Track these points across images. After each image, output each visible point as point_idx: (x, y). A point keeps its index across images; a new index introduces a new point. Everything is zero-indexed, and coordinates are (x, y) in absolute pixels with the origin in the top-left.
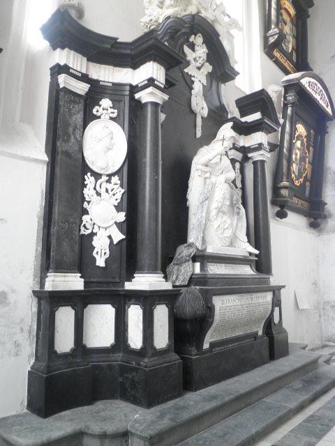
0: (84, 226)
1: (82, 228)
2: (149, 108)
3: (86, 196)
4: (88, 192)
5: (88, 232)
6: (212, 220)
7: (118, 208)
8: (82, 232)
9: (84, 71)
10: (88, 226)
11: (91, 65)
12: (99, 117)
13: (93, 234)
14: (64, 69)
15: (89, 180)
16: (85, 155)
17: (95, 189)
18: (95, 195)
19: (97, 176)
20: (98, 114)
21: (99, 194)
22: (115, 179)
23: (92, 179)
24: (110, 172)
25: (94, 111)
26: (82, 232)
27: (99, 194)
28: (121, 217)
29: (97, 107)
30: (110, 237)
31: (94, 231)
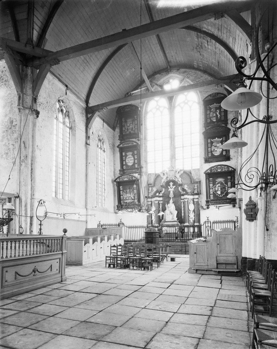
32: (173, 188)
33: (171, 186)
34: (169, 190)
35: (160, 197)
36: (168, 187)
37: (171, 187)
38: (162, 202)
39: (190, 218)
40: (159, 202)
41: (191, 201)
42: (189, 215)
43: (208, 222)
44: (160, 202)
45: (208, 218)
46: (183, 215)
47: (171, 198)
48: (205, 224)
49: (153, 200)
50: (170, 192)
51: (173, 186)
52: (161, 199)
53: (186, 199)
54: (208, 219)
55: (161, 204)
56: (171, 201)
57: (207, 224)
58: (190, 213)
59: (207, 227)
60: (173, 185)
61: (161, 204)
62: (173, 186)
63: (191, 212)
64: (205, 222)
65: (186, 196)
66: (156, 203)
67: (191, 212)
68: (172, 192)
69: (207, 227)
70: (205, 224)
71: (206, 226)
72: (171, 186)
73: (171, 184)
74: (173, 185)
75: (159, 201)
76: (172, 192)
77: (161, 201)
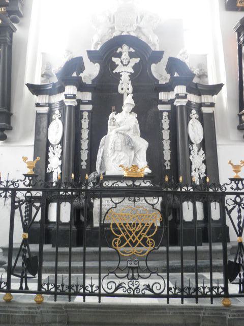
0: (49, 169)
2: (67, 108)
4: (50, 154)
5: (50, 171)
6: (110, 156)
7: (60, 159)
8: (47, 172)
9: (47, 102)
10: (50, 169)
11: (51, 97)
14: (38, 105)
15: (51, 149)
16: (49, 138)
21: (54, 154)
22: (60, 146)
23: (52, 148)
24: (57, 143)
26: (47, 172)
27: (54, 154)
28: (60, 163)
32: (132, 64)
33: (125, 56)
34: (116, 70)
36: (114, 59)
39: (193, 167)
40: (77, 108)
41: (194, 111)
42: (191, 157)
44: (83, 107)
50: (118, 76)
51: (131, 58)
52: (88, 96)
55: (86, 115)
58: (192, 152)
60: (131, 55)
61: (86, 115)
62: (131, 58)
63: (195, 148)
67: (195, 148)
72: (125, 56)
73: (125, 50)
74: (131, 55)
75: (80, 102)
77: (89, 103)
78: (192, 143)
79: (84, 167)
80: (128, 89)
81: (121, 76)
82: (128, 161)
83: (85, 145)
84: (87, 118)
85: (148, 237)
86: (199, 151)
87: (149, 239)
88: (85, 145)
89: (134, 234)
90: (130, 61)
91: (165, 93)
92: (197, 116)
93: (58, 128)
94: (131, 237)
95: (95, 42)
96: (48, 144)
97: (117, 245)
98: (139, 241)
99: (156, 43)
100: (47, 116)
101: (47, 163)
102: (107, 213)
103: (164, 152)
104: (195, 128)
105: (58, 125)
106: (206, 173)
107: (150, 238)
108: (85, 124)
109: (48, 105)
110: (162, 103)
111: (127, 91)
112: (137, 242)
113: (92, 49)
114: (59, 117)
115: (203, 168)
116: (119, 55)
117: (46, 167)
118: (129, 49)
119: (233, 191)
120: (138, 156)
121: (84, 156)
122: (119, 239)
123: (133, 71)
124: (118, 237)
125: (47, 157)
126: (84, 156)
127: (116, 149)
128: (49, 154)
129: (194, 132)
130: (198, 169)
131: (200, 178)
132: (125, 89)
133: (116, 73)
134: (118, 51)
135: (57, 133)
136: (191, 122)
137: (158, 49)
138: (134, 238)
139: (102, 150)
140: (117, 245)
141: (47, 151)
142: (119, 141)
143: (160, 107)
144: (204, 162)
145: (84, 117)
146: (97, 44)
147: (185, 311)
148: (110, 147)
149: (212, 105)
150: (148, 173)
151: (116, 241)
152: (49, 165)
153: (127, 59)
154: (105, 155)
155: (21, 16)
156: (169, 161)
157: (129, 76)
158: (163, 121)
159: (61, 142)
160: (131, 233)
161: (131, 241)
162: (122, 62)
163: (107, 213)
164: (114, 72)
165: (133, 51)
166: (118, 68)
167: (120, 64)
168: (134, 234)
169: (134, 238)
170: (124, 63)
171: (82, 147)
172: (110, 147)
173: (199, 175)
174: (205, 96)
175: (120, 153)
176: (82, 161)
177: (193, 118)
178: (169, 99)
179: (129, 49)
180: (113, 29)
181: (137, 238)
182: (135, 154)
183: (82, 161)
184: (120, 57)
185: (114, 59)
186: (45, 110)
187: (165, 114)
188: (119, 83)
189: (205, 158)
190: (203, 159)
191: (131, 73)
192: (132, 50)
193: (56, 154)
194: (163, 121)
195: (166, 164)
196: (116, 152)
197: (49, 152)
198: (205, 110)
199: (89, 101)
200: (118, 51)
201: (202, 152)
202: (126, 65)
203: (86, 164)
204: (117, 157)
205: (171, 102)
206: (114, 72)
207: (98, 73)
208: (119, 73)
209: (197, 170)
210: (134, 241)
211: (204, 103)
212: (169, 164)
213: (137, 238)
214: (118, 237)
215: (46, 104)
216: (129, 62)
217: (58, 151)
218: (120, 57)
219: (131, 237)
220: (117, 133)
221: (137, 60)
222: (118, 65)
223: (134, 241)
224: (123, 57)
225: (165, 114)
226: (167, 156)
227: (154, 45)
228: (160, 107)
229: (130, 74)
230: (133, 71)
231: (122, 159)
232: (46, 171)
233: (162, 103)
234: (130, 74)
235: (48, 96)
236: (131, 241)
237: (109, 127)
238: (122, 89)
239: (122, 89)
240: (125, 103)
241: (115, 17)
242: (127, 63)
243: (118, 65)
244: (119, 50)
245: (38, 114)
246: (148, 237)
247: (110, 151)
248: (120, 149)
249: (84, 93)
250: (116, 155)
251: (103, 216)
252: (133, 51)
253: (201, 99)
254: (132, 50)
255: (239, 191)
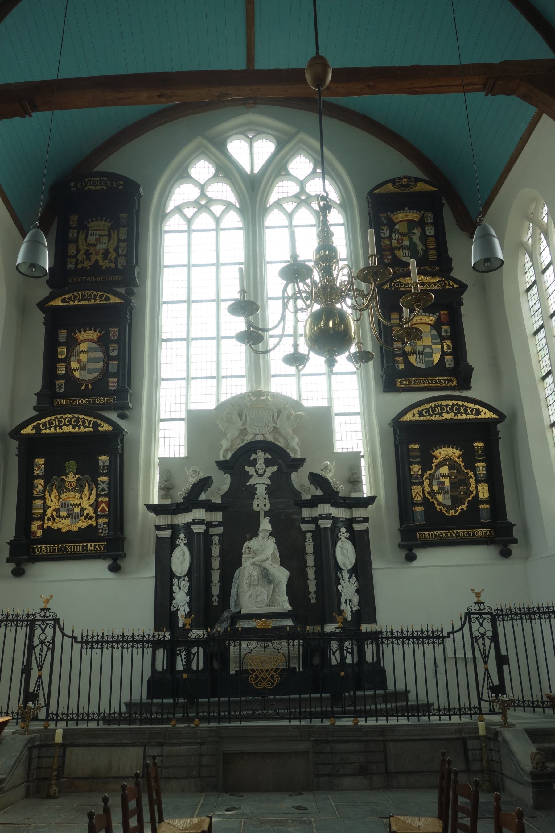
0: (173, 606)
1: (172, 608)
3: (174, 590)
4: (175, 588)
5: (176, 609)
6: (245, 591)
7: (187, 594)
8: (172, 610)
9: (169, 523)
11: (174, 516)
12: (179, 545)
13: (178, 610)
14: (158, 528)
15: (175, 581)
17: (178, 585)
18: (178, 589)
19: (179, 578)
20: (179, 543)
21: (180, 588)
22: (186, 579)
23: (177, 580)
24: (183, 575)
25: (177, 543)
26: (172, 610)
27: (180, 588)
29: (178, 540)
30: (185, 611)
31: (178, 608)
32: (269, 473)
33: (260, 464)
34: (251, 482)
35: (209, 506)
36: (247, 468)
37: (261, 472)
38: (220, 530)
39: (343, 600)
40: (207, 531)
41: (343, 530)
42: (340, 587)
43: (480, 614)
44: (213, 531)
45: (478, 595)
46: (312, 587)
47: (259, 512)
48: (466, 628)
49: (188, 518)
51: (267, 467)
52: (218, 516)
53: (329, 517)
54: (479, 603)
55: (216, 539)
56: (265, 525)
57: (475, 626)
58: (341, 581)
59: (480, 641)
60: (268, 463)
61: (216, 539)
62: (267, 467)
63: (346, 574)
64: (468, 614)
65: (325, 509)
66: (199, 533)
68: (261, 491)
69: (480, 641)
70: (466, 628)
71: (476, 634)
72: (260, 464)
73: (260, 456)
74: (268, 463)
75: (209, 525)
76: (261, 491)
77: (219, 525)
78: (341, 570)
79: (215, 604)
80: (265, 505)
81: (257, 488)
82: (266, 597)
83: (216, 576)
84: (218, 543)
85: (275, 674)
86: (350, 578)
87: (275, 676)
88: (216, 576)
89: (264, 672)
90: (266, 470)
91: (308, 509)
92: (347, 535)
93: (184, 556)
94: (262, 674)
95: (224, 448)
96: (172, 575)
97: (253, 680)
98: (269, 677)
99: (296, 447)
100: (169, 540)
101: (172, 599)
102: (245, 656)
103: (308, 582)
104: (345, 550)
105: (184, 553)
106: (359, 604)
107: (276, 674)
108: (215, 551)
109: (170, 527)
110: (305, 521)
111: (263, 508)
112: (267, 677)
113: (221, 459)
114: (185, 542)
115: (356, 599)
116: (254, 463)
117: (171, 603)
118: (265, 454)
119: (476, 611)
120: (277, 590)
121: (216, 590)
122: (254, 676)
123: (270, 483)
124: (253, 674)
125: (172, 592)
126: (216, 590)
127: (251, 583)
128: (174, 587)
129: (344, 555)
130: (350, 601)
131: (352, 612)
132: (261, 505)
133: (250, 485)
134: (252, 458)
135: (183, 562)
136: (339, 543)
137: (299, 457)
138: (265, 675)
139: (236, 585)
140: (253, 680)
141: (172, 585)
142: (255, 573)
143: (304, 527)
144: (357, 591)
145: (214, 542)
146: (227, 450)
147: (301, 727)
148: (245, 581)
149: (365, 520)
150: (289, 611)
151: (252, 677)
152: (174, 602)
153: (262, 469)
154: (240, 590)
155: (129, 408)
156: (314, 592)
157: (266, 488)
158: (306, 544)
159: (189, 574)
160: (262, 671)
161: (262, 678)
162: (256, 471)
163: (245, 656)
164: (248, 484)
165: (270, 457)
166: (252, 480)
167: (255, 474)
168: (264, 672)
169: (265, 675)
170: (260, 473)
171: (213, 579)
172: (245, 581)
173: (351, 608)
174: (357, 509)
175: (257, 588)
176: (213, 596)
177: (343, 538)
178: (313, 516)
179: (265, 454)
180: (244, 431)
181: (267, 675)
182: (274, 588)
183: (213, 596)
184: (254, 466)
185: (247, 468)
186: (167, 533)
187: (309, 535)
188: (254, 498)
189: (358, 587)
190: (356, 588)
191: (267, 485)
192: (268, 456)
193: (182, 588)
194: (306, 544)
195: (310, 596)
196: (252, 586)
197: (174, 585)
198: (357, 527)
199: (219, 522)
200: (252, 458)
201: (354, 579)
202: (262, 475)
203: (217, 599)
204: (253, 591)
205: (314, 520)
206: (248, 484)
207: (229, 487)
208: (254, 485)
209: (348, 601)
210: (265, 677)
211: (355, 518)
212: (315, 596)
213: (267, 675)
214: (253, 674)
215: (168, 525)
216: (265, 472)
217: (185, 584)
218: (254, 466)
219: (262, 674)
220: (252, 564)
221: (275, 469)
222: (252, 476)
223: (265, 677)
224: (258, 466)
225: (309, 535)
226: (312, 587)
227: (294, 450)
228: (304, 527)
229: (267, 486)
230: (270, 483)
231: (259, 595)
232: (171, 609)
233: (305, 521)
234: (267, 486)
235: (170, 516)
236: (262, 678)
237: (243, 556)
238: (258, 505)
239: (258, 505)
240: (261, 528)
241: (247, 414)
242: (262, 473)
243: (252, 476)
244: (253, 456)
245: (158, 539)
246: (275, 674)
247: (245, 586)
248: (256, 583)
249: (213, 513)
250: (252, 590)
251: (242, 659)
252: (270, 457)
253: (352, 513)
254: (268, 456)
255: (481, 612)
